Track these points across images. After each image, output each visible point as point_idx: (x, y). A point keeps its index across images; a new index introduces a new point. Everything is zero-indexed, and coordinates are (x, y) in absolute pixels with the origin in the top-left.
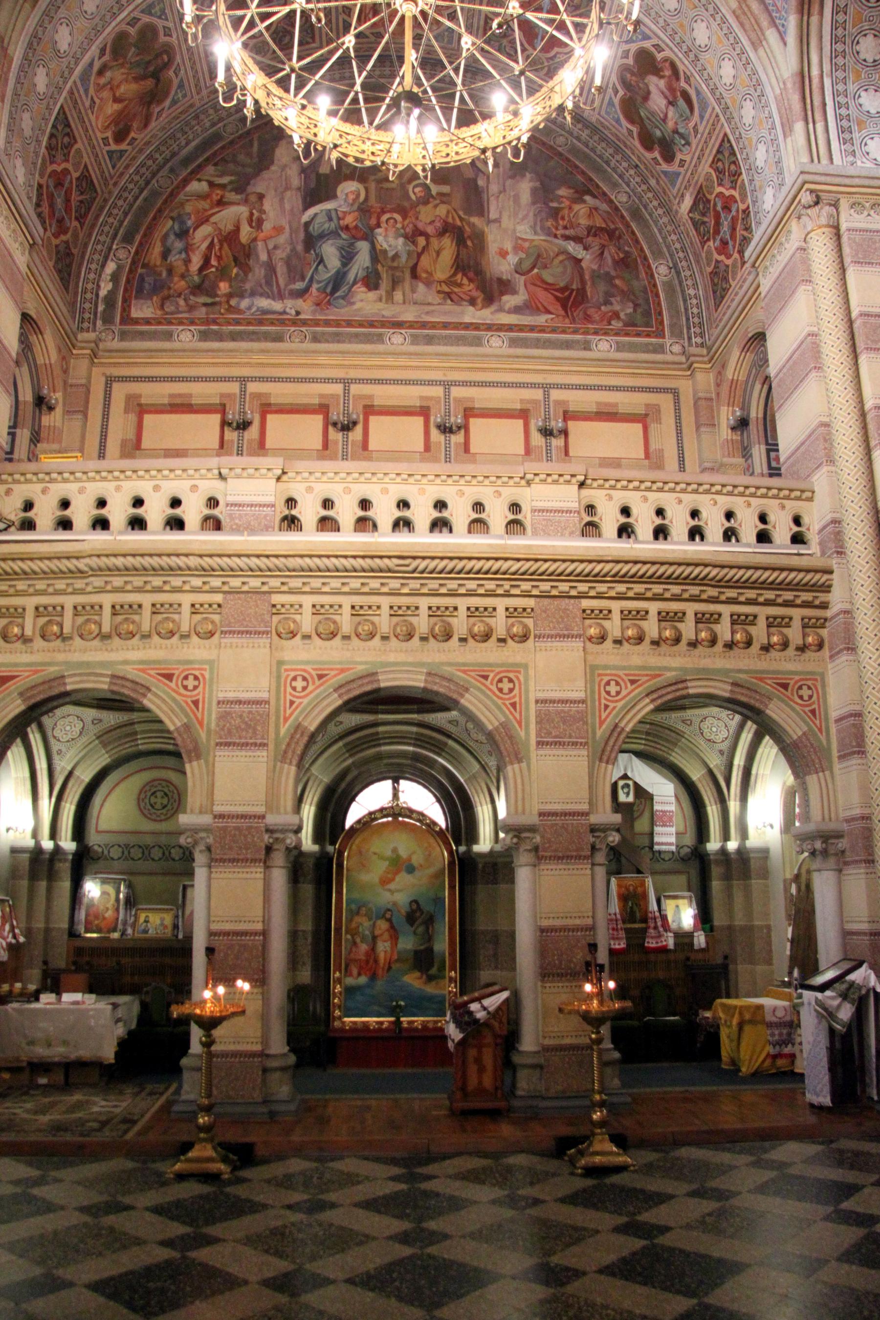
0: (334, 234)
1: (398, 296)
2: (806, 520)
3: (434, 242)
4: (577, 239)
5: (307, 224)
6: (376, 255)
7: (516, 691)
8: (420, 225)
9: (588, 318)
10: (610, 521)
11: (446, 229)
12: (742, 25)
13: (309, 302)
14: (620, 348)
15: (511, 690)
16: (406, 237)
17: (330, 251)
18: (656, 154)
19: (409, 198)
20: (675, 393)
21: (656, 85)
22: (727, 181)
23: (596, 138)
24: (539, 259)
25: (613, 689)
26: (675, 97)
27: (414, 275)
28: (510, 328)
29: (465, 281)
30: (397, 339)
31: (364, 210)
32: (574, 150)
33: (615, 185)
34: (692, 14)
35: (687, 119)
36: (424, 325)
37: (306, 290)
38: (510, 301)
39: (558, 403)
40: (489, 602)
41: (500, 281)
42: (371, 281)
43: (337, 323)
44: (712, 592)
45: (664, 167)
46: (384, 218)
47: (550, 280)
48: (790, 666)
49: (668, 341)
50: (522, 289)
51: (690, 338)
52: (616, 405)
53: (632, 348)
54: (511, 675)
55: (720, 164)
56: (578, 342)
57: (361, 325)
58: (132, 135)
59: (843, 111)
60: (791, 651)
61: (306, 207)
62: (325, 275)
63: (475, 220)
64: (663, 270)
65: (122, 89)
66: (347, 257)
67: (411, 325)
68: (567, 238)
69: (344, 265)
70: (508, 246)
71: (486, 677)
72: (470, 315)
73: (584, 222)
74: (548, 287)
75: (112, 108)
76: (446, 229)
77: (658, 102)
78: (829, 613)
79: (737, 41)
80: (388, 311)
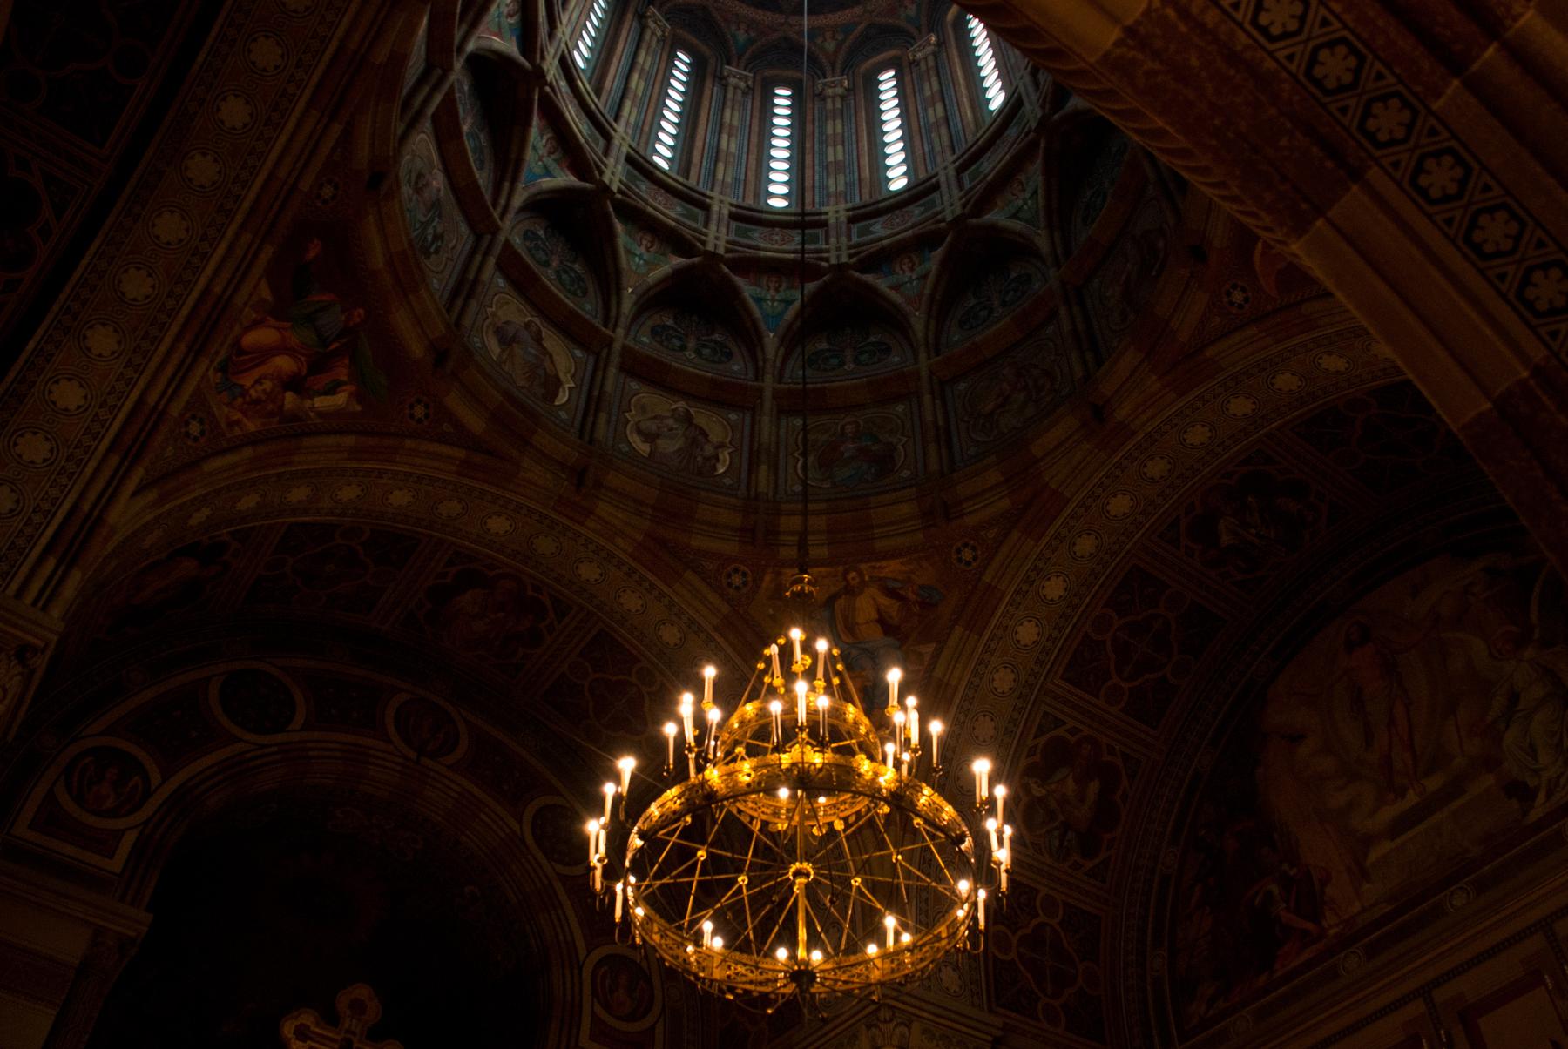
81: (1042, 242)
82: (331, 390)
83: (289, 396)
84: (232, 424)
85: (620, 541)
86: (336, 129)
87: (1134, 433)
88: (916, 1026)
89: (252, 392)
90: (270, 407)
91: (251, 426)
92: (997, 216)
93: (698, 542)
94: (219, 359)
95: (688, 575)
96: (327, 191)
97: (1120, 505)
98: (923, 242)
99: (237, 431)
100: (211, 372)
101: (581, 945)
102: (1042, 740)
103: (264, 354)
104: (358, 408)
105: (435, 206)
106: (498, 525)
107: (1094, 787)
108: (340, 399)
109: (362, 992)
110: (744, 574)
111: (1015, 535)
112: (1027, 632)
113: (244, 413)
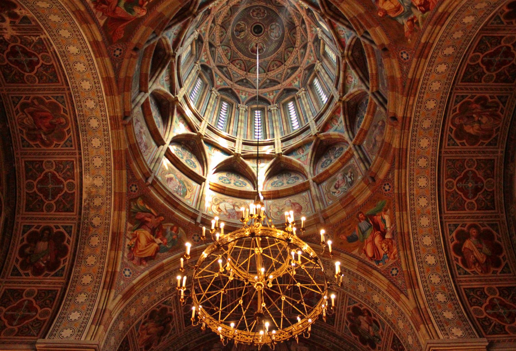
12: (390, 294)
18: (368, 346)
21: (363, 319)
23: (342, 342)
26: (371, 323)
34: (371, 292)
35: (378, 330)
55: (395, 346)
58: (152, 347)
59: (438, 319)
65: (151, 330)
75: (146, 337)
77: (365, 326)
79: (390, 300)
82: (384, 220)
83: (388, 236)
84: (395, 258)
85: (411, 102)
89: (386, 250)
90: (390, 243)
91: (395, 250)
94: (375, 265)
95: (410, 76)
99: (396, 256)
100: (379, 267)
103: (375, 248)
104: (389, 210)
105: (344, 176)
106: (424, 143)
108: (386, 217)
110: (402, 53)
113: (391, 253)
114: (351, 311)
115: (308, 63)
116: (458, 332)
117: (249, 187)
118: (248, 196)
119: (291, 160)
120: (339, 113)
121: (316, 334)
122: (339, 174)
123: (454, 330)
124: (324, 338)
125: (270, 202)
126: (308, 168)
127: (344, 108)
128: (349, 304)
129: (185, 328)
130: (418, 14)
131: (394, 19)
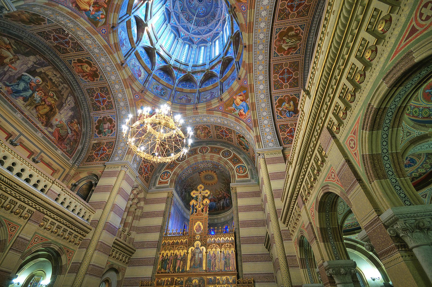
0: (27, 83)
1: (28, 108)
2: (91, 217)
3: (46, 106)
4: (71, 130)
5: (23, 75)
6: (31, 96)
7: (14, 232)
8: (46, 100)
9: (61, 145)
10: (61, 200)
11: (50, 106)
13: (6, 89)
14: (62, 154)
15: (13, 231)
16: (41, 99)
17: (22, 85)
18: (97, 131)
19: (49, 94)
20: (65, 170)
22: (107, 147)
24: (62, 127)
25: (36, 240)
27: (36, 107)
28: (45, 134)
29: (45, 118)
30: (19, 116)
31: (38, 86)
32: (83, 115)
33: (84, 127)
36: (28, 118)
37: (9, 86)
38: (50, 129)
39: (41, 156)
40: (26, 205)
41: (51, 124)
42: (25, 99)
43: (8, 100)
44: (70, 225)
45: (96, 134)
46: (40, 91)
47: (61, 132)
48: (71, 247)
49: (71, 160)
50: (54, 129)
51: (75, 162)
52: (52, 165)
53: (64, 156)
54: (16, 227)
56: (55, 147)
57: (14, 105)
60: (73, 244)
61: (26, 72)
62: (16, 88)
63: (57, 110)
64: (80, 147)
66: (25, 90)
67: (25, 116)
68: (70, 128)
69: (23, 90)
70: (59, 120)
71: (10, 225)
72: (40, 125)
73: (75, 128)
74: (59, 133)
76: (50, 106)
78: (84, 238)
80: (23, 108)
81: (239, 29)
86: (130, 89)
87: (252, 45)
88: (265, 154)
92: (235, 31)
93: (213, 107)
95: (214, 112)
96: (137, 97)
97: (261, 57)
98: (230, 44)
101: (233, 167)
102: (277, 101)
105: (162, 89)
107: (292, 103)
109: (201, 185)
111: (248, 74)
112: (261, 87)
114: (108, 118)
115: (193, 38)
116: (135, 166)
117: (135, 39)
118: (132, 43)
119: (155, 56)
120: (184, 73)
121: (83, 105)
122: (161, 86)
123: (135, 165)
124: (84, 109)
125: (135, 57)
126: (156, 68)
127: (186, 75)
128: (112, 116)
129: (35, 33)
130: (237, 112)
131: (234, 103)
